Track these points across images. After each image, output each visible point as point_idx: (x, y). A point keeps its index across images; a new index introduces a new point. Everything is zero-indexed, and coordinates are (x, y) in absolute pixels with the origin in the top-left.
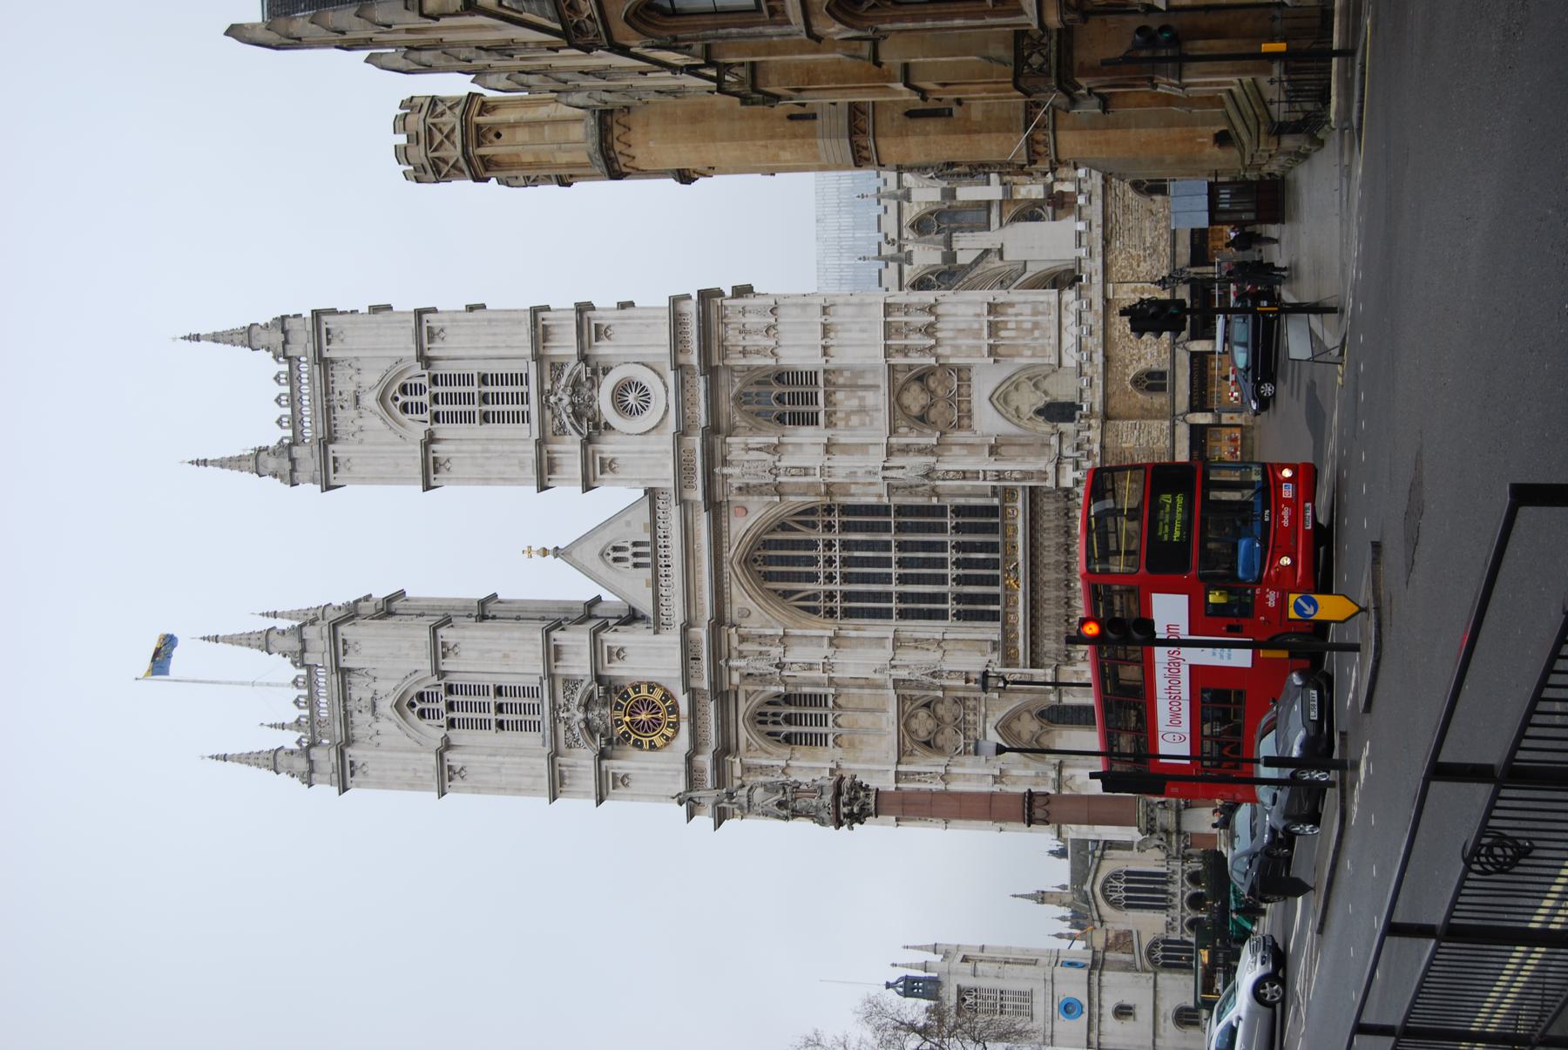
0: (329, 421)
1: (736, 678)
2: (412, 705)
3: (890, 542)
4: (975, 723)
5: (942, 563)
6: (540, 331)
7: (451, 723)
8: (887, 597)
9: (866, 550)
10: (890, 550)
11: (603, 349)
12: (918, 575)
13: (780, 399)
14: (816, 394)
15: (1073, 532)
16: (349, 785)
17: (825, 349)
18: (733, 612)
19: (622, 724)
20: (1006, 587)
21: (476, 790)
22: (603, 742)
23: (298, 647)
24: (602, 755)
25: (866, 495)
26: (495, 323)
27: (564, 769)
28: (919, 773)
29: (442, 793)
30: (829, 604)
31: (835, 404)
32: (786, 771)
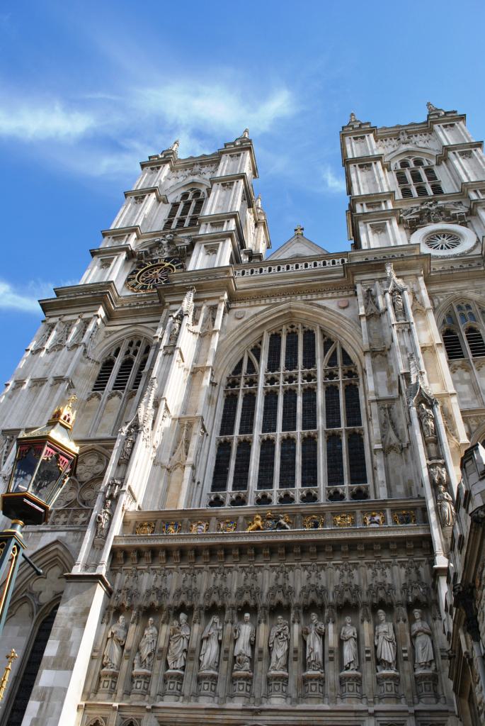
0: (388, 136)
2: (192, 189)
3: (315, 427)
4: (72, 523)
5: (287, 480)
7: (176, 205)
8: (247, 426)
9: (304, 410)
10: (304, 428)
13: (471, 330)
15: (348, 619)
16: (145, 168)
18: (239, 308)
20: (249, 518)
24: (131, 255)
25: (376, 383)
27: (127, 237)
30: (242, 382)
31: (479, 370)
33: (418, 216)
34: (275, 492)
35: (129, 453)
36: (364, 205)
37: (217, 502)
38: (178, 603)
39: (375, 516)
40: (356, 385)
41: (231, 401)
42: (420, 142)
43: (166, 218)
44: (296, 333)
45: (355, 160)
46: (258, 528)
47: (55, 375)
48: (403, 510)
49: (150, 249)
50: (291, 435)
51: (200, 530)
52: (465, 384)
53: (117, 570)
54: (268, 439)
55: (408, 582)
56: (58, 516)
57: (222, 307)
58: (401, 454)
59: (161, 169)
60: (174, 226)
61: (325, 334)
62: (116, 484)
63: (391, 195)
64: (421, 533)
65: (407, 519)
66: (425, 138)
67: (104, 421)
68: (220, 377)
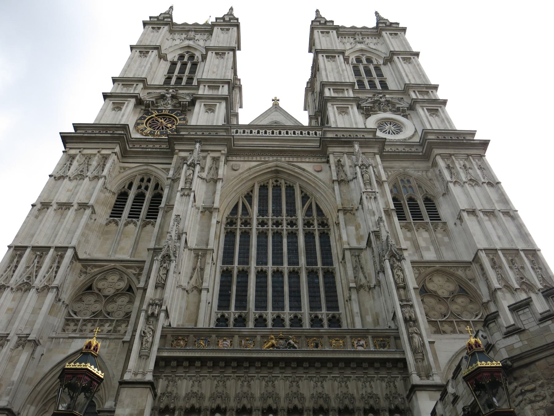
1: (183, 154)
2: (187, 52)
5: (278, 305)
6: (424, 90)
7: (174, 64)
9: (288, 249)
10: (289, 264)
11: (422, 112)
12: (266, 287)
13: (411, 199)
14: (423, 220)
16: (147, 27)
17: (472, 212)
18: (236, 162)
19: (158, 112)
21: (131, 59)
22: (148, 102)
23: (227, 19)
24: (139, 102)
26: (422, 76)
27: (135, 86)
28: (58, 267)
29: (132, 48)
32: (96, 180)
33: (372, 105)
34: (270, 314)
35: (164, 278)
36: (332, 90)
37: (222, 321)
38: (214, 406)
39: (359, 341)
40: (327, 234)
41: (230, 235)
42: (371, 43)
43: (166, 74)
44: (280, 186)
45: (323, 51)
46: (273, 346)
47: (80, 202)
48: (380, 337)
49: (156, 100)
50: (280, 269)
51: (226, 345)
52: (408, 241)
53: (158, 376)
54: (262, 270)
55: (388, 393)
56: (85, 325)
57: (223, 159)
58: (369, 291)
59: (161, 29)
60: (173, 81)
61: (303, 190)
62: (156, 304)
63: (352, 85)
64: (398, 356)
65: (384, 344)
66: (375, 41)
67: (123, 244)
68: (221, 216)
